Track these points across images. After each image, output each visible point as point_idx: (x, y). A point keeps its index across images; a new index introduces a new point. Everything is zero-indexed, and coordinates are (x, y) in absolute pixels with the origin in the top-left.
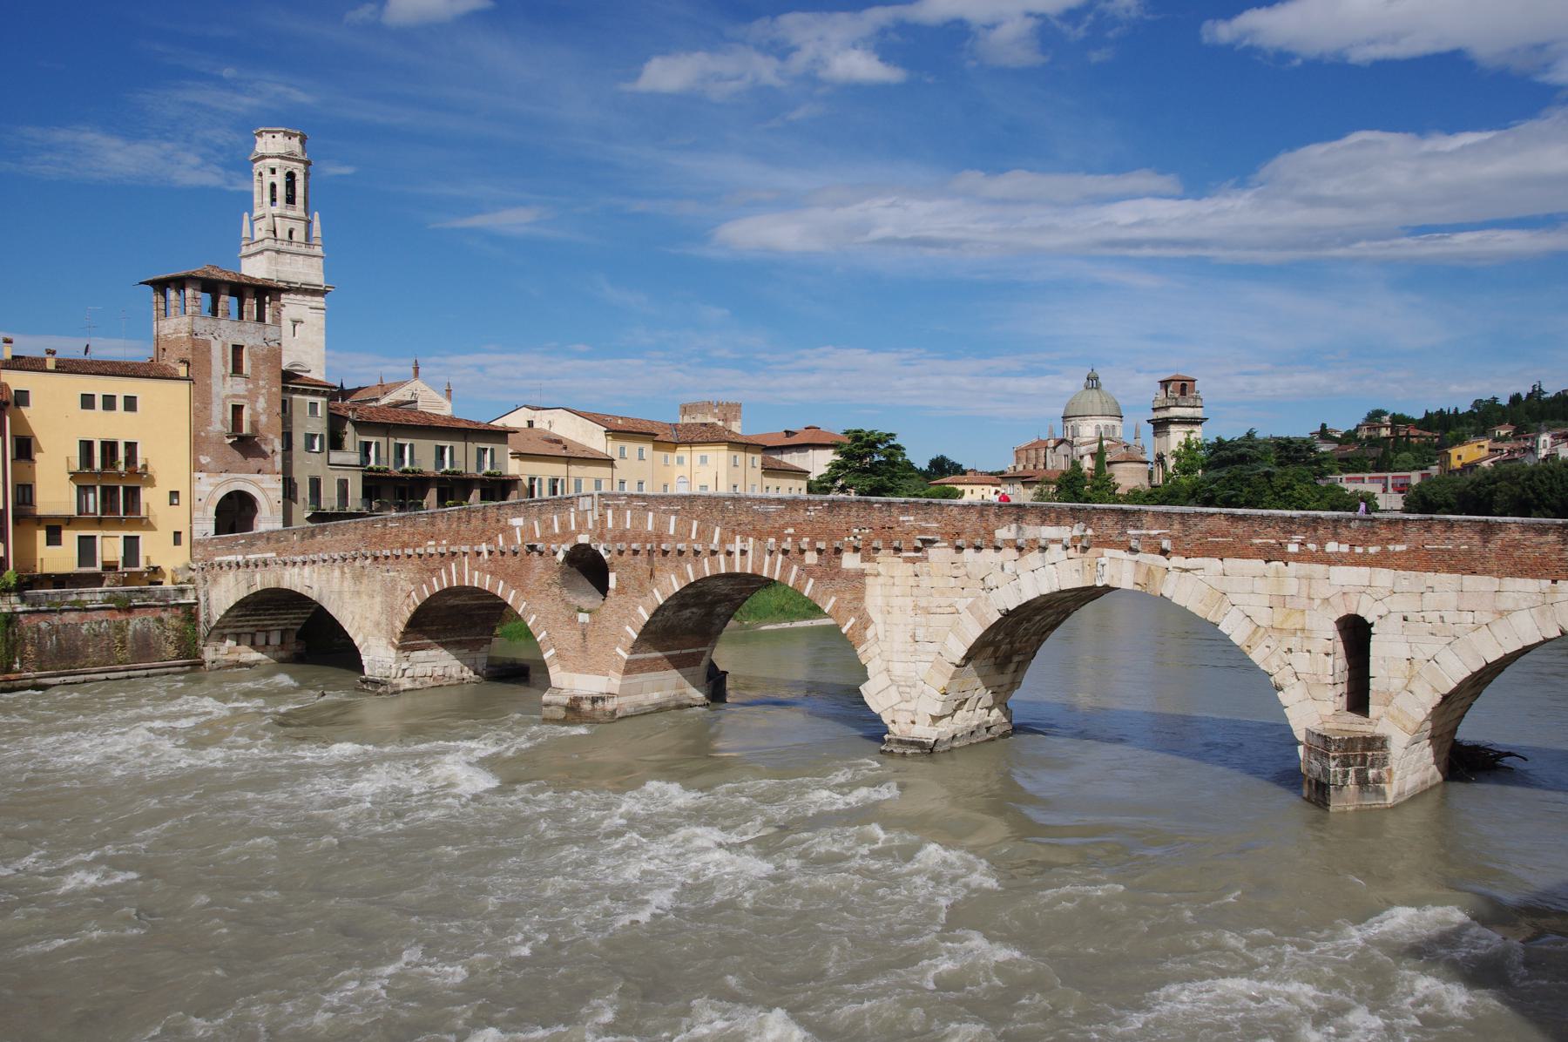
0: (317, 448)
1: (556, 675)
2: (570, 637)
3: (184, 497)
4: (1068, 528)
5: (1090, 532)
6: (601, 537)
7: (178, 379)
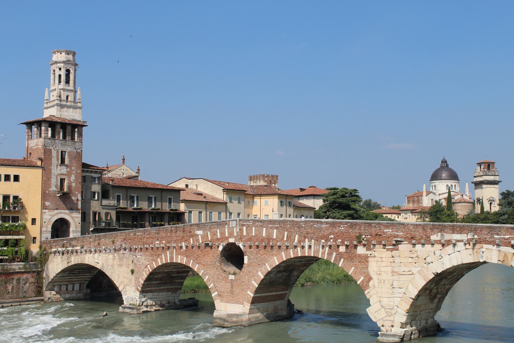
0: (96, 198)
1: (218, 304)
2: (225, 287)
3: (38, 222)
4: (466, 235)
5: (476, 237)
6: (241, 239)
7: (37, 167)
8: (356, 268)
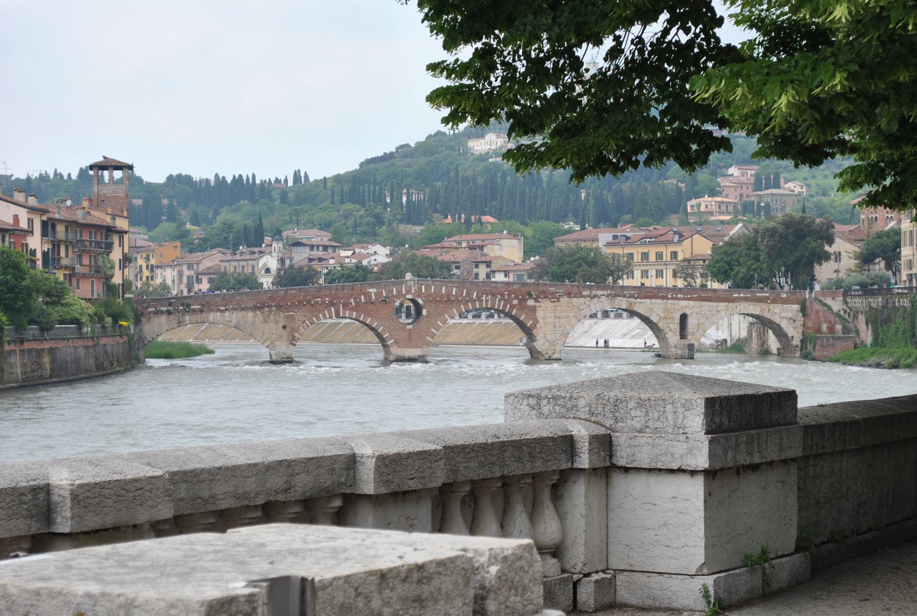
6: (419, 296)
8: (527, 315)
